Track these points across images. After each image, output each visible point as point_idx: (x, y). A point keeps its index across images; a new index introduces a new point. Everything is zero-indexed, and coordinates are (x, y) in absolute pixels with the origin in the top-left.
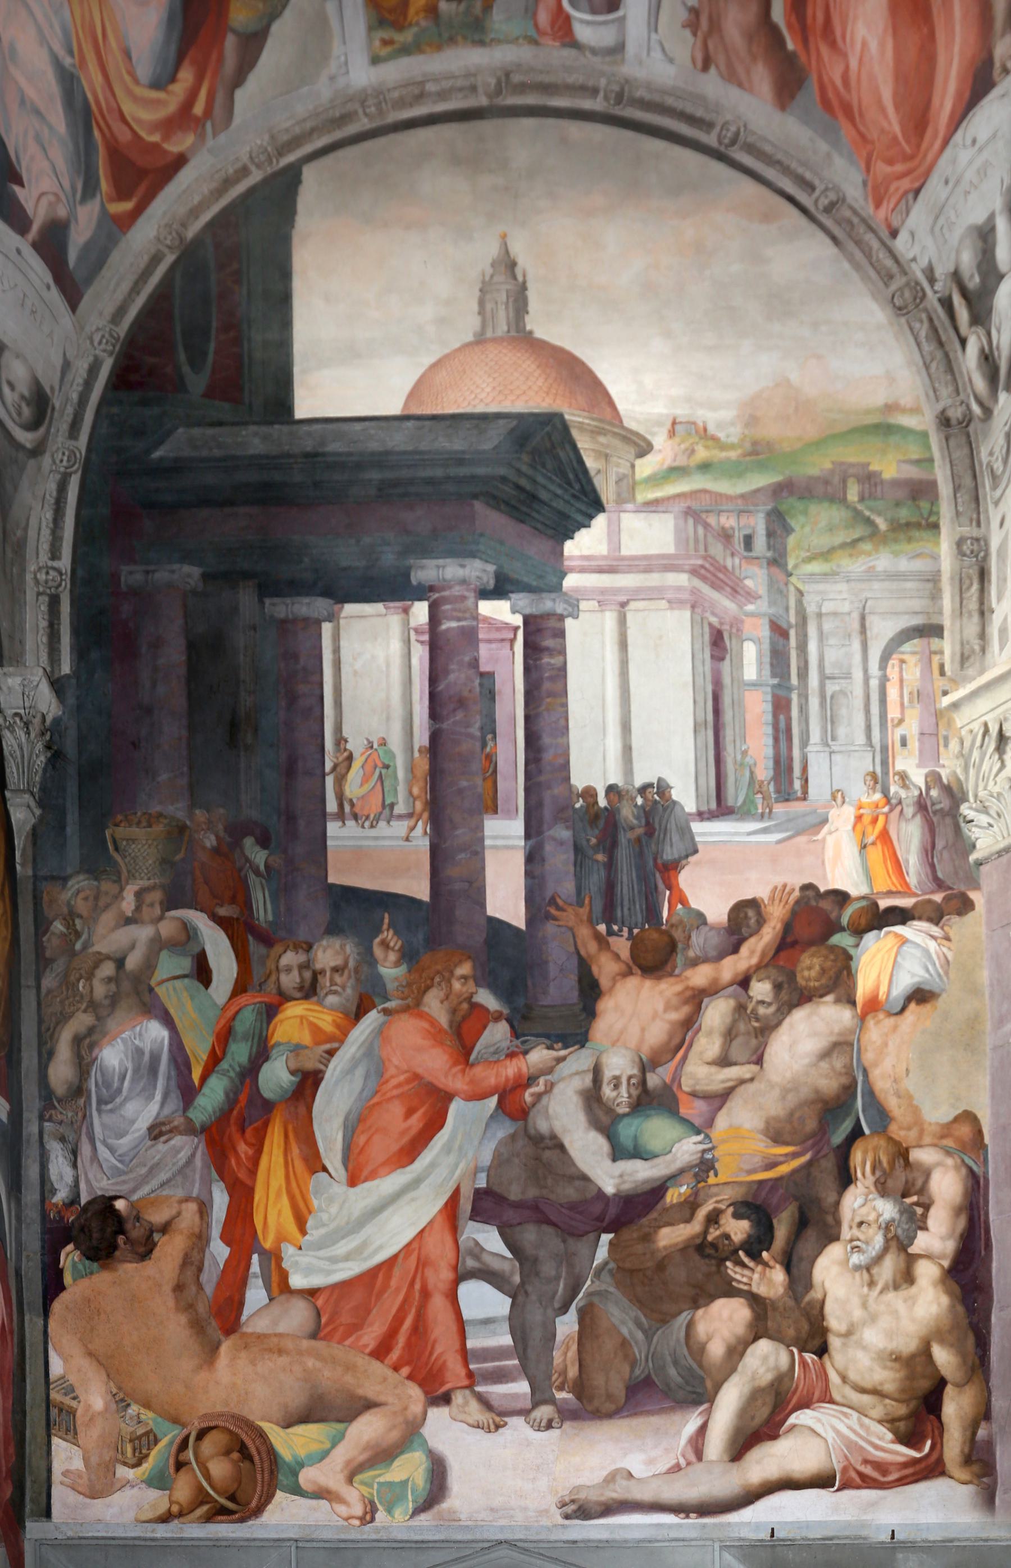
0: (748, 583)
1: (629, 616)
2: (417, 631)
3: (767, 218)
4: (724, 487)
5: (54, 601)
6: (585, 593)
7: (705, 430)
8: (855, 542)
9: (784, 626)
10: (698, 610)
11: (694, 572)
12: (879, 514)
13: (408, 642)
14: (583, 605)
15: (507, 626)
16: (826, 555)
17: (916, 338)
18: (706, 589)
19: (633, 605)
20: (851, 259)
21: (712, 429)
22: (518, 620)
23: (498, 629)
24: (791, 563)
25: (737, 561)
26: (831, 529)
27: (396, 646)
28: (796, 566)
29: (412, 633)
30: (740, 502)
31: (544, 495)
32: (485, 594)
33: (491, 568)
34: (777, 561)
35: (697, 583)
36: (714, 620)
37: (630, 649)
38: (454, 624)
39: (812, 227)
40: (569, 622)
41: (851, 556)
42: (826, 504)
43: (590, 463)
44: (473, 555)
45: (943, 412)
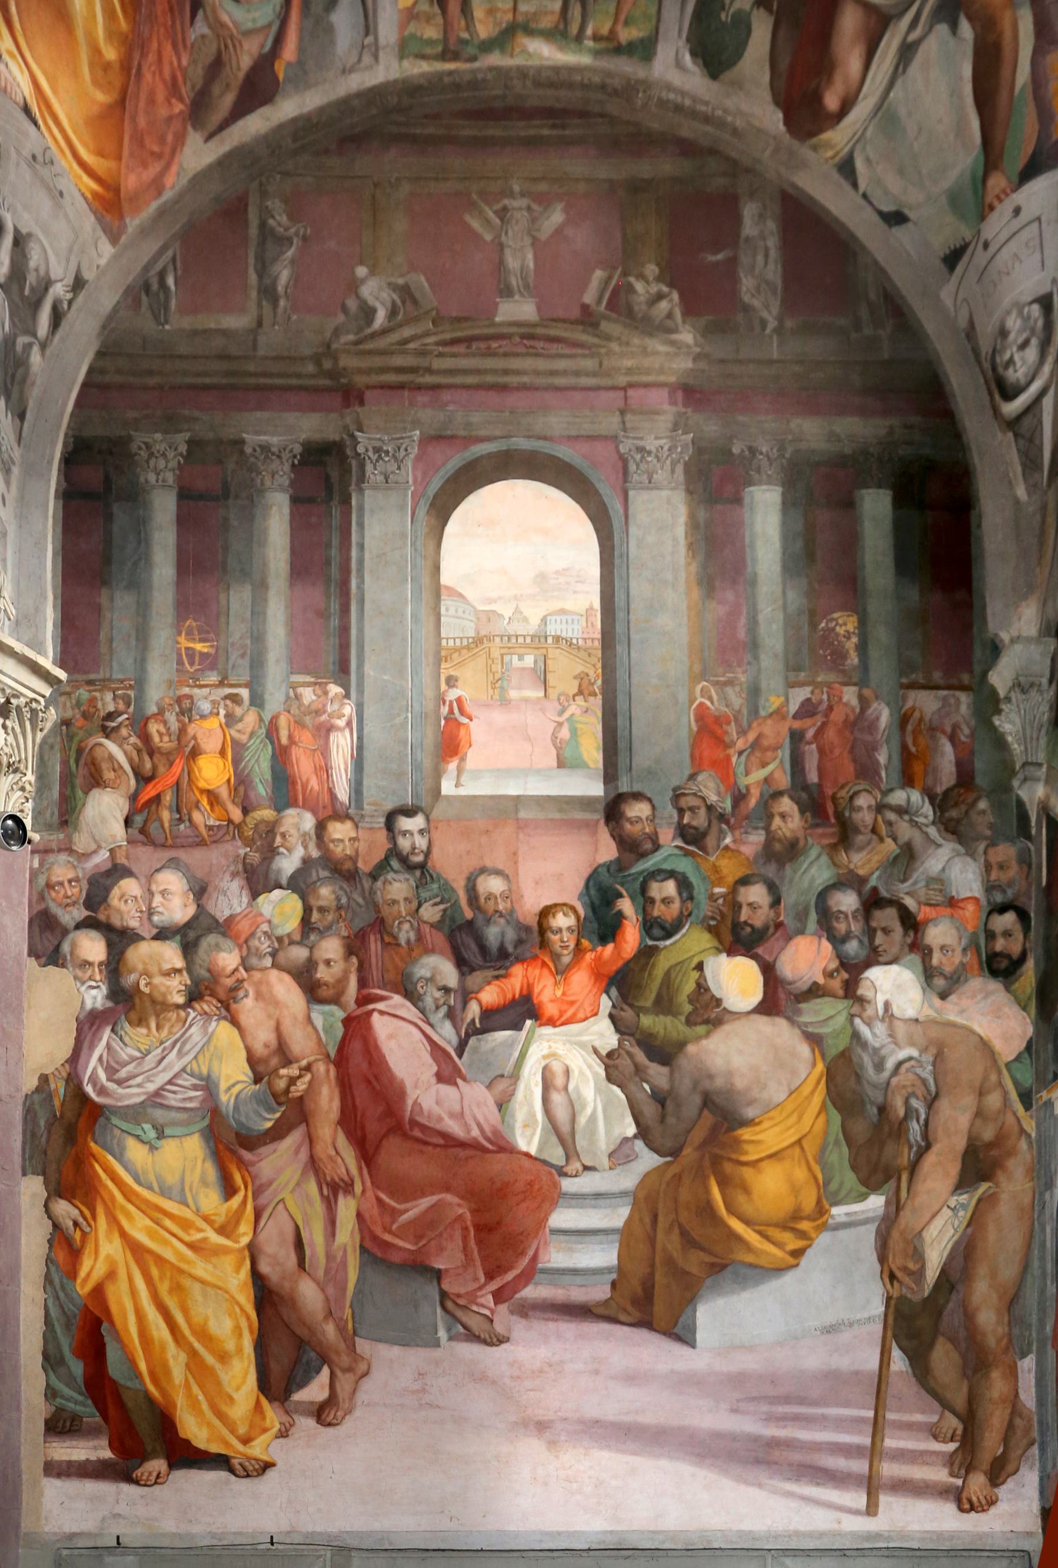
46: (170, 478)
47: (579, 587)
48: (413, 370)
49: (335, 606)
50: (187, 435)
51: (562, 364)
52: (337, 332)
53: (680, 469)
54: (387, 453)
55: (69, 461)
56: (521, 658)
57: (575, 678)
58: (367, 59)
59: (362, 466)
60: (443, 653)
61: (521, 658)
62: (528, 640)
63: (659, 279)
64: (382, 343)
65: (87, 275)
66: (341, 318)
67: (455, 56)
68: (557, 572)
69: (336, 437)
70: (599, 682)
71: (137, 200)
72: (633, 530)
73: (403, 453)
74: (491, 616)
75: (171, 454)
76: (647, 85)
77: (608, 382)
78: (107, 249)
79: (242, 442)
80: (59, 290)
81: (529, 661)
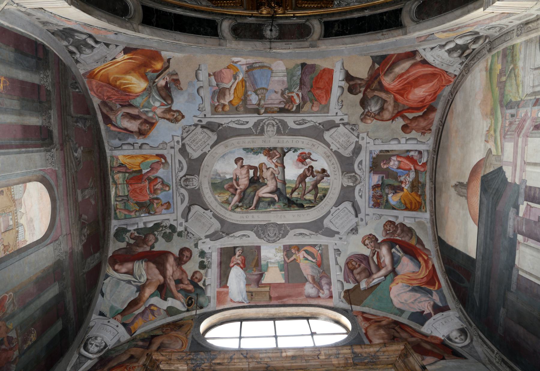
0: (522, 116)
1: (528, 161)
2: (524, 241)
3: (453, 112)
4: (500, 125)
5: (503, 360)
6: (521, 176)
7: (488, 131)
8: (515, 76)
9: (535, 100)
10: (529, 134)
11: (519, 136)
12: (509, 68)
13: (527, 246)
14: (524, 178)
15: (526, 207)
16: (518, 86)
17: (474, 64)
18: (523, 131)
19: (525, 159)
20: (460, 87)
21: (487, 129)
22: (525, 203)
23: (527, 211)
24: (519, 100)
25: (517, 120)
26: (511, 85)
27: (528, 250)
28: (520, 97)
29: (525, 243)
30: (503, 119)
31: (497, 187)
32: (517, 213)
33: (512, 209)
34: (517, 105)
35: (521, 135)
36: (532, 128)
37: (537, 162)
38: (524, 227)
39: (454, 99)
40: (529, 184)
41: (518, 77)
42: (506, 88)
43: (492, 170)
44: (508, 214)
45: (488, 51)
46: (42, 83)
47: (31, 235)
48: (68, 165)
49: (18, 142)
50: (51, 90)
51: (72, 212)
52: (72, 141)
53: (58, 258)
54: (53, 159)
55: (44, 46)
56: (12, 219)
57: (8, 243)
58: (110, 148)
59: (49, 151)
60: (9, 187)
61: (12, 219)
62: (16, 221)
63: (88, 235)
64: (72, 155)
65: (78, 64)
66: (75, 143)
67: (111, 170)
68: (33, 225)
69: (54, 142)
70: (8, 253)
71: (90, 83)
72: (45, 248)
73: (53, 164)
74: (21, 204)
75: (47, 83)
76: (110, 219)
77: (71, 227)
78: (82, 72)
79: (51, 110)
80: (78, 55)
81: (11, 223)
